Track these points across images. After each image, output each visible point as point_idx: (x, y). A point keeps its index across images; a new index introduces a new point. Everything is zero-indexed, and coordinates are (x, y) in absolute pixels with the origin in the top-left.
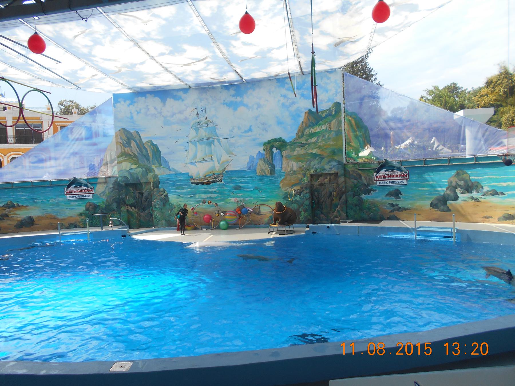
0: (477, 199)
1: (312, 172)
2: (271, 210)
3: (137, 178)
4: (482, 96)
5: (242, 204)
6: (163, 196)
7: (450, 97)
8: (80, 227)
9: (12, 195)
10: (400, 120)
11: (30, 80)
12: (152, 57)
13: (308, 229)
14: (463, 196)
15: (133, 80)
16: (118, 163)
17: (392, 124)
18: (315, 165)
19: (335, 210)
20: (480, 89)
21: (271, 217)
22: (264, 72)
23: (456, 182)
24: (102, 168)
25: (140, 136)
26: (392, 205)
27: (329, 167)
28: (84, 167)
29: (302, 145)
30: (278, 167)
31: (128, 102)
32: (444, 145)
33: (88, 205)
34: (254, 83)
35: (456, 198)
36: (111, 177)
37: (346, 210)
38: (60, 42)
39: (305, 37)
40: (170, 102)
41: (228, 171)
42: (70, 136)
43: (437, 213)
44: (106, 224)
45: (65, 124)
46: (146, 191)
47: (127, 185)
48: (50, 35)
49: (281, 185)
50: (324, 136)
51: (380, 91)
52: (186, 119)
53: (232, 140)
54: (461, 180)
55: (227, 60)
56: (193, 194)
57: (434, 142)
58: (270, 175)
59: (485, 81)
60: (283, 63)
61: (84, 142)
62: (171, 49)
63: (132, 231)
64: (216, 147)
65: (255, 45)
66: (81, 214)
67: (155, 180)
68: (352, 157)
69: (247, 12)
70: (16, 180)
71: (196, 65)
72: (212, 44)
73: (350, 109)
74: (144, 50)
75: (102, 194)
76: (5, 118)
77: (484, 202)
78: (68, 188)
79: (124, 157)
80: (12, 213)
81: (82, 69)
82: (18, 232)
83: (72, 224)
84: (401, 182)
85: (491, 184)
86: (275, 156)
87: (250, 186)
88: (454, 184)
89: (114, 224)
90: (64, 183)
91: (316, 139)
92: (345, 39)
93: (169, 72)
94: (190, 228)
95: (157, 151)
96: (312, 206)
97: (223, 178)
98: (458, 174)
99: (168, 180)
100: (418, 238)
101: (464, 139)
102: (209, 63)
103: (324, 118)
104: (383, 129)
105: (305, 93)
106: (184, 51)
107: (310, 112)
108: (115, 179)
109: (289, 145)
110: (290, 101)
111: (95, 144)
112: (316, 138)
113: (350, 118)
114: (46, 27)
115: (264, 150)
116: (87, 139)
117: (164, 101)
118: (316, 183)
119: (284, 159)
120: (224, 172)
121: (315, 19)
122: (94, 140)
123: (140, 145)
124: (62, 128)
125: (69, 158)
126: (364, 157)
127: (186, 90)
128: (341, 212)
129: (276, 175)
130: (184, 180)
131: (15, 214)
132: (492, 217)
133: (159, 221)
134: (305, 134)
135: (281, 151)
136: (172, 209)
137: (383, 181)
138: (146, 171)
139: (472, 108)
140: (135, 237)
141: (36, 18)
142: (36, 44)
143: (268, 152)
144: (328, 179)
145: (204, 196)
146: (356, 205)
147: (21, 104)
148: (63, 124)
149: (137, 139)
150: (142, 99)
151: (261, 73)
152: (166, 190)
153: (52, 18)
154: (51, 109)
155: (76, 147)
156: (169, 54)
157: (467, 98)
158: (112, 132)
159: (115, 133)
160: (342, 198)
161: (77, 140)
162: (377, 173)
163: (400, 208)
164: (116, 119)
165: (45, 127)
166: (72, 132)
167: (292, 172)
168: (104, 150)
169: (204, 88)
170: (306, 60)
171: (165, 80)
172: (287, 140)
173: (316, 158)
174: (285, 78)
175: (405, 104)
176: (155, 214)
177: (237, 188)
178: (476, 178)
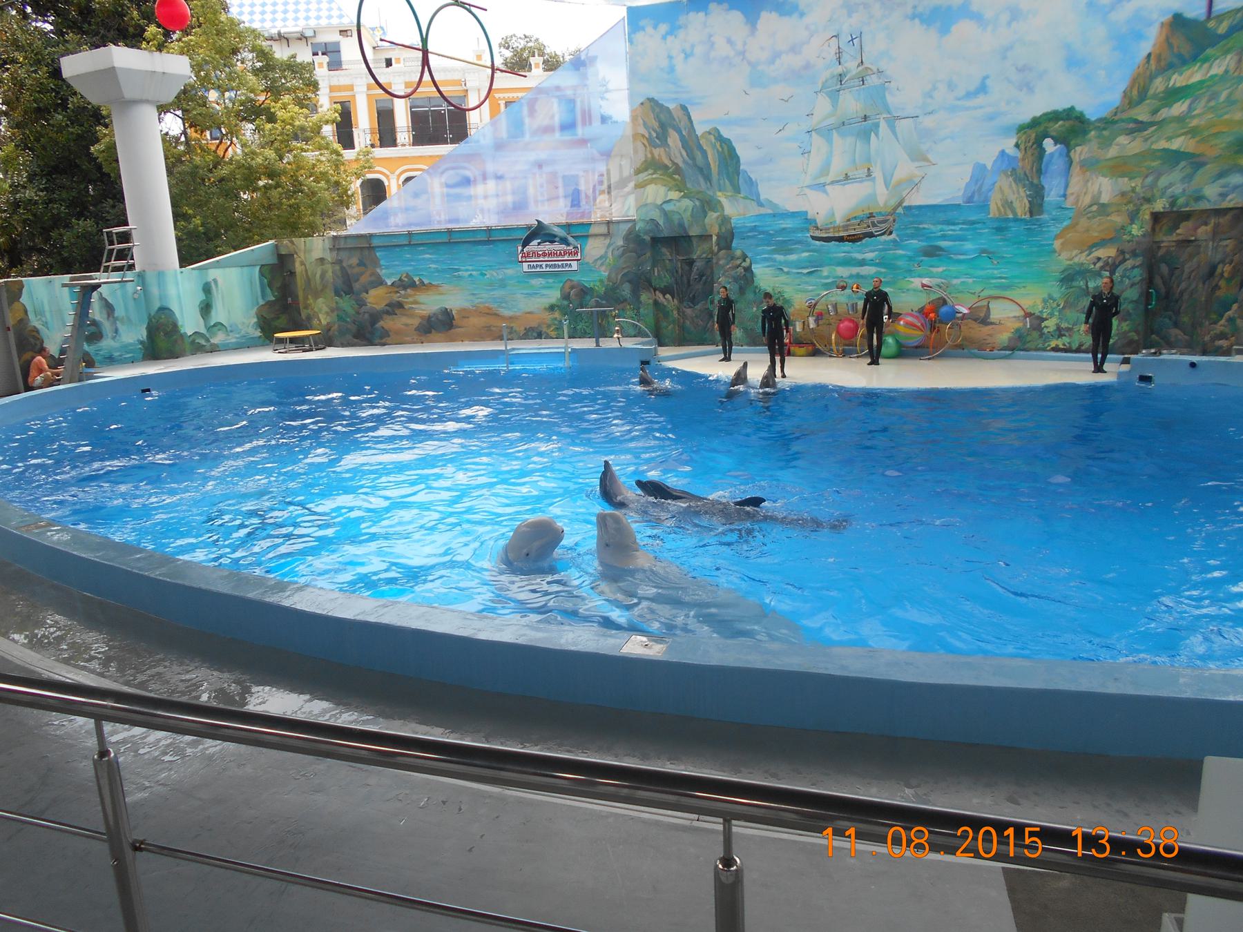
1: (1159, 206)
2: (1022, 313)
3: (681, 225)
6: (740, 270)
8: (548, 337)
13: (1125, 368)
16: (637, 186)
18: (1171, 185)
19: (1222, 316)
21: (1017, 330)
24: (600, 198)
25: (690, 118)
28: (558, 198)
29: (1139, 127)
31: (663, 28)
33: (568, 285)
36: (618, 222)
41: (909, 208)
42: (527, 120)
44: (604, 333)
45: (515, 95)
46: (699, 257)
47: (656, 241)
49: (1057, 244)
52: (807, 66)
53: (928, 122)
56: (814, 267)
61: (557, 135)
63: (664, 352)
66: (552, 308)
75: (599, 262)
78: (524, 246)
79: (650, 171)
80: (411, 299)
83: (532, 329)
87: (969, 246)
94: (803, 350)
95: (729, 157)
96: (1148, 302)
97: (896, 226)
99: (754, 229)
108: (630, 225)
109: (1096, 128)
111: (583, 142)
115: (1017, 146)
118: (1167, 240)
119: (1076, 169)
120: (900, 210)
122: (580, 131)
123: (691, 143)
124: (507, 104)
129: (1045, 217)
130: (794, 231)
131: (416, 302)
135: (1069, 151)
140: (670, 364)
143: (1029, 153)
144: (1209, 228)
149: (683, 124)
152: (749, 255)
159: (632, 111)
161: (548, 130)
164: (633, 74)
165: (472, 101)
166: (532, 112)
167: (1094, 208)
168: (607, 155)
172: (1092, 114)
173: (1178, 164)
177: (933, 252)
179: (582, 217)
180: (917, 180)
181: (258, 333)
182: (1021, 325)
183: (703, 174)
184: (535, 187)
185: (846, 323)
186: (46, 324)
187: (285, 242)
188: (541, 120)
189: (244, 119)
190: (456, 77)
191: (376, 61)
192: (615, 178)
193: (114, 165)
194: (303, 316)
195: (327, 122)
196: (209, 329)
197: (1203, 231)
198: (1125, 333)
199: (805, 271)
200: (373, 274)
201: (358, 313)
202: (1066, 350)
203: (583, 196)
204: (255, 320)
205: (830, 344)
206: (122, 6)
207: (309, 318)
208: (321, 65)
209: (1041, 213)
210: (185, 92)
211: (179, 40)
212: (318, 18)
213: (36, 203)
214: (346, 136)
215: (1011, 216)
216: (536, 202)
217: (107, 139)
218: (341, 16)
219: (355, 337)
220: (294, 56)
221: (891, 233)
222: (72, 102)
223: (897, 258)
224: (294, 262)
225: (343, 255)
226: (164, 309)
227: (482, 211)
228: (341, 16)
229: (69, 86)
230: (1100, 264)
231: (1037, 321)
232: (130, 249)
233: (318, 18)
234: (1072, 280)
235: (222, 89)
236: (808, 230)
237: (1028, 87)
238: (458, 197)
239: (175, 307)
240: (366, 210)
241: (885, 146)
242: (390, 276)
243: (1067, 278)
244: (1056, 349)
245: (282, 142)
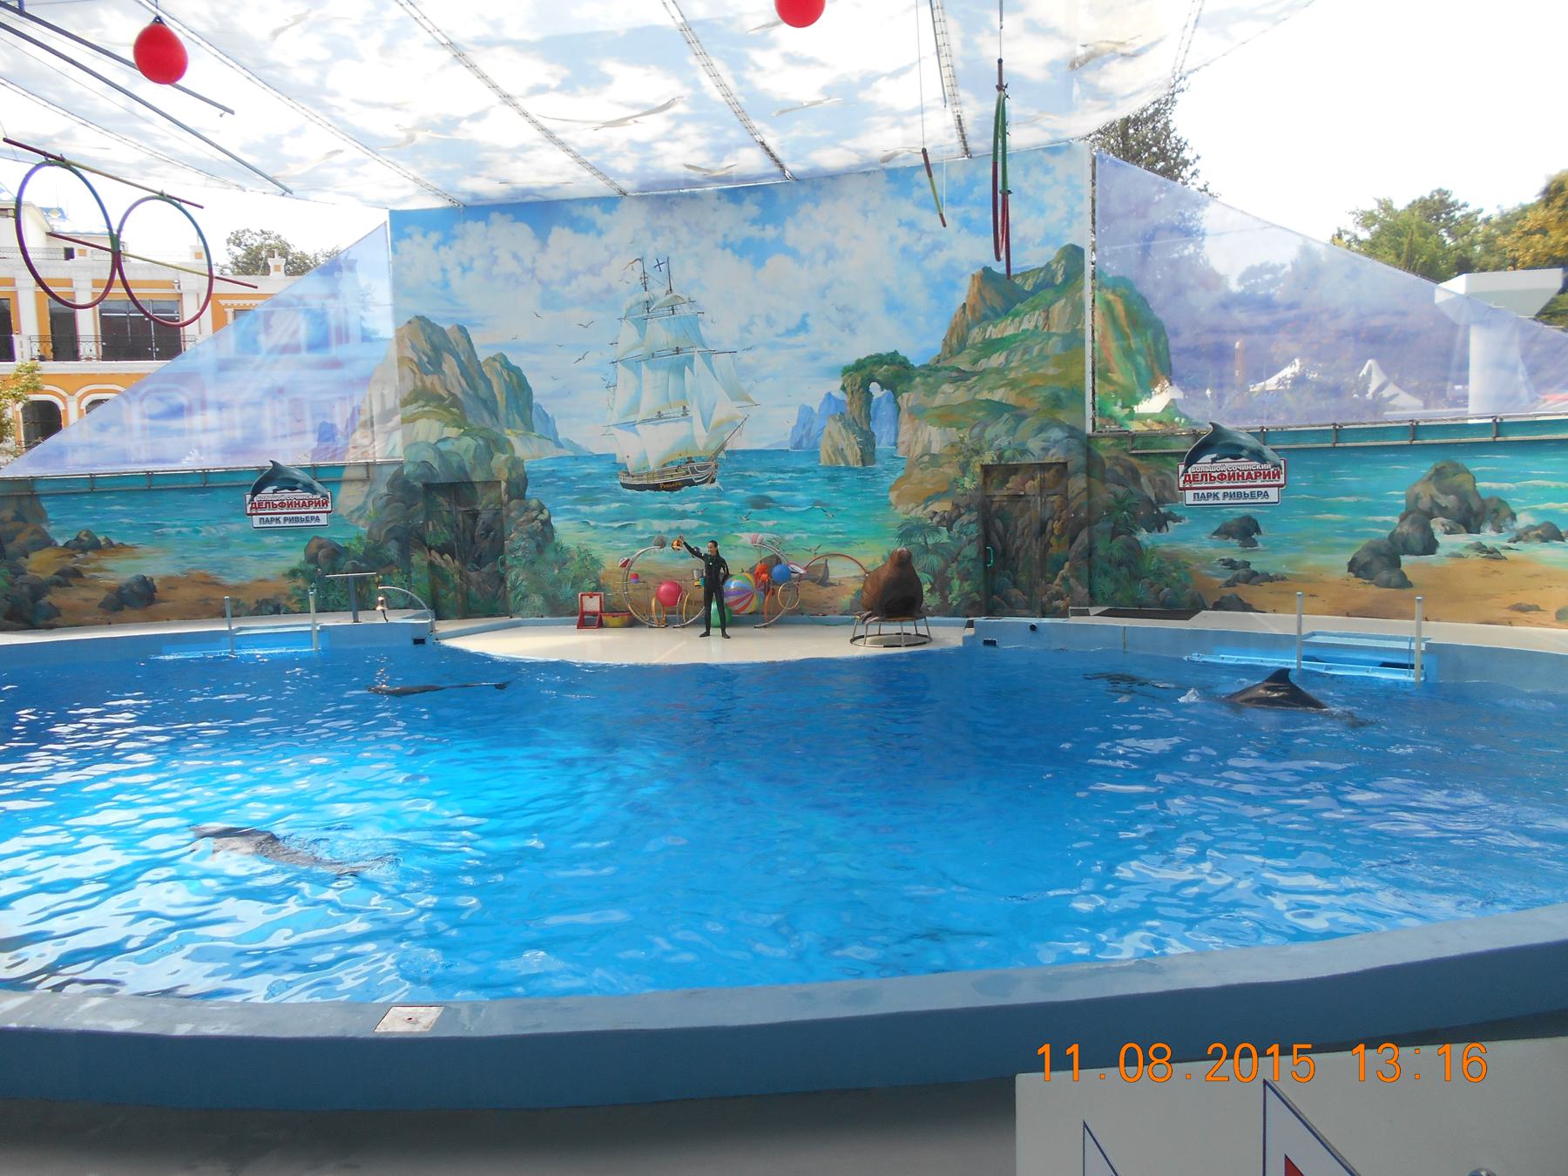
0: (1493, 551)
1: (989, 458)
3: (462, 468)
4: (1529, 233)
6: (537, 524)
7: (1426, 233)
8: (289, 612)
9: (90, 513)
10: (1267, 304)
11: (143, 168)
12: (507, 98)
13: (971, 631)
14: (1451, 543)
15: (448, 167)
16: (404, 421)
17: (1241, 317)
18: (997, 437)
20: (1525, 209)
23: (1432, 498)
24: (358, 435)
25: (469, 341)
26: (1230, 564)
27: (1041, 445)
28: (302, 433)
29: (962, 376)
30: (884, 440)
31: (435, 237)
32: (1399, 384)
34: (820, 184)
35: (1430, 547)
36: (382, 464)
37: (1090, 577)
38: (228, 47)
39: (979, 40)
40: (561, 237)
41: (733, 453)
42: (262, 338)
43: (1369, 592)
44: (365, 604)
45: (248, 302)
46: (485, 508)
47: (430, 488)
48: (201, 27)
49: (892, 496)
51: (1207, 211)
52: (609, 290)
53: (746, 358)
54: (1446, 493)
55: (736, 108)
56: (626, 520)
57: (1369, 372)
58: (860, 466)
59: (1542, 184)
60: (907, 120)
61: (306, 356)
63: (443, 627)
64: (698, 378)
65: (823, 65)
66: (293, 573)
67: (514, 474)
68: (1111, 417)
71: (640, 125)
72: (692, 60)
73: (1112, 268)
74: (483, 77)
76: (69, 283)
77: (1514, 562)
78: (254, 494)
79: (421, 403)
80: (93, 565)
81: (297, 133)
82: (109, 623)
83: (266, 602)
84: (1259, 494)
85: (1541, 507)
86: (877, 408)
87: (800, 497)
88: (1425, 503)
89: (391, 605)
90: (246, 479)
91: (1002, 359)
92: (1104, 45)
93: (561, 144)
94: (616, 621)
95: (519, 388)
96: (986, 561)
98: (1439, 473)
99: (552, 474)
100: (1306, 665)
101: (1464, 366)
102: (680, 120)
103: (1032, 293)
104: (1214, 330)
106: (607, 80)
107: (987, 275)
108: (395, 468)
110: (927, 240)
111: (336, 364)
113: (1111, 297)
115: (843, 388)
116: (312, 347)
117: (542, 236)
118: (999, 494)
119: (904, 417)
120: (722, 455)
122: (335, 351)
123: (471, 370)
124: (238, 312)
125: (258, 404)
126: (1151, 416)
127: (608, 203)
128: (1072, 581)
129: (878, 466)
130: (600, 477)
131: (101, 569)
132: (1537, 608)
133: (525, 597)
134: (970, 342)
137: (1205, 491)
138: (488, 447)
139: (1497, 268)
142: (159, 55)
143: (857, 396)
144: (1036, 483)
145: (660, 526)
146: (1120, 564)
147: (115, 239)
148: (242, 302)
149: (462, 347)
150: (475, 228)
152: (547, 505)
155: (280, 373)
156: (559, 89)
157: (1480, 238)
158: (384, 324)
161: (285, 349)
162: (1188, 465)
163: (1255, 574)
164: (398, 287)
165: (189, 309)
166: (267, 327)
167: (926, 458)
168: (366, 381)
169: (666, 198)
170: (978, 110)
171: (548, 172)
172: (916, 361)
175: (1284, 255)
176: (512, 576)
177: (761, 503)
178: (1494, 485)
179: (333, 457)
183: (487, 409)
184: (271, 417)
188: (280, 336)
191: (48, 250)
192: (376, 410)
197: (1031, 486)
198: (968, 594)
199: (616, 525)
200: (37, 532)
201: (12, 584)
205: (649, 611)
209: (873, 462)
219: (8, 617)
223: (722, 509)
227: (200, 448)
230: (937, 519)
237: (850, 328)
242: (61, 534)
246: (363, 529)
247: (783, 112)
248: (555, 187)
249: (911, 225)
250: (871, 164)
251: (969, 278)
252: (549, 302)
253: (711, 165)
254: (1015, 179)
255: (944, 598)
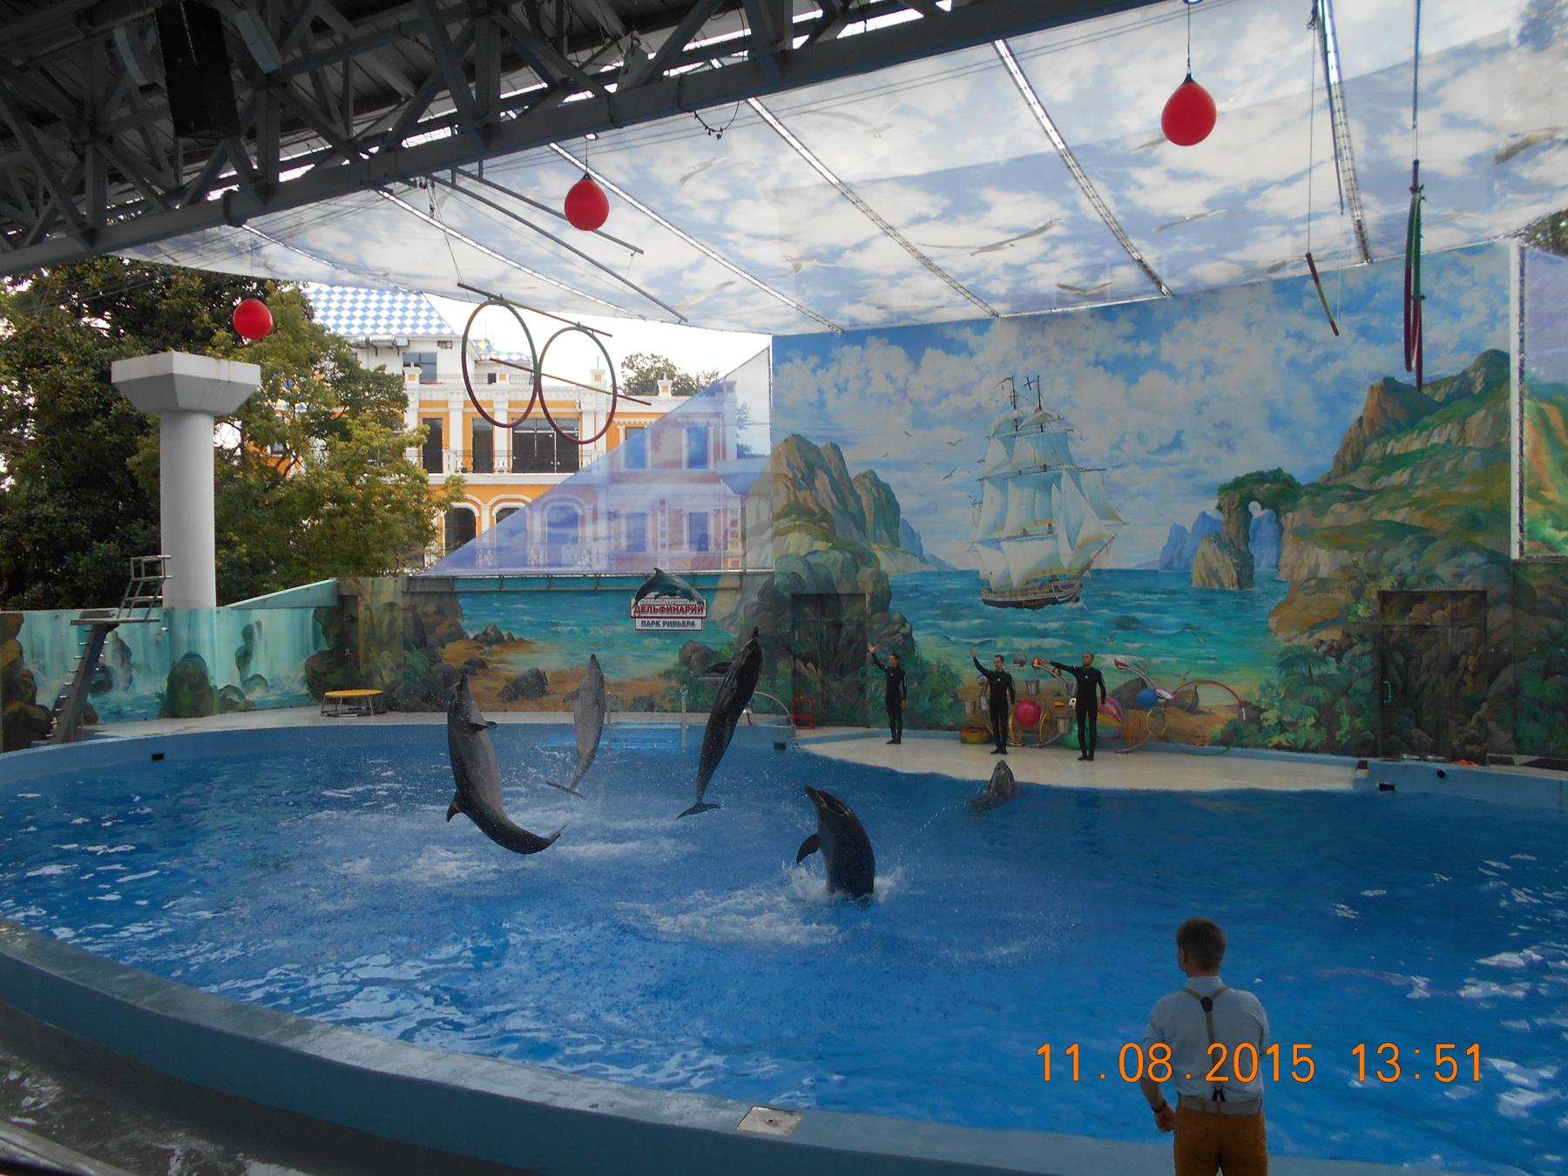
1: (1387, 584)
2: (1235, 702)
3: (829, 581)
5: (1138, 674)
9: (499, 610)
12: (889, 230)
13: (1362, 773)
15: (830, 294)
16: (775, 534)
18: (1398, 561)
19: (1470, 717)
21: (1232, 722)
22: (1232, 262)
27: (1449, 571)
28: (681, 543)
29: (1356, 495)
30: (1264, 562)
31: (814, 360)
34: (1199, 300)
36: (754, 574)
39: (1386, 140)
40: (933, 358)
41: (1098, 572)
42: (649, 454)
47: (797, 598)
48: (622, 179)
49: (1272, 622)
50: (1437, 467)
52: (979, 408)
53: (1117, 476)
56: (987, 635)
58: (1236, 588)
60: (1299, 227)
61: (685, 468)
62: (946, 202)
63: (803, 734)
65: (1208, 178)
66: (668, 674)
69: (1189, 77)
70: (509, 571)
72: (1071, 183)
74: (867, 211)
76: (491, 404)
78: (638, 599)
81: (695, 267)
83: (642, 699)
87: (1169, 619)
91: (1405, 476)
93: (938, 271)
94: (975, 737)
95: (887, 503)
96: (1383, 697)
97: (1084, 591)
99: (915, 588)
102: (1056, 242)
105: (1375, 322)
107: (1389, 386)
108: (766, 579)
109: (1308, 493)
110: (1319, 351)
111: (715, 478)
112: (1408, 471)
113: (1544, 406)
114: (608, 159)
115: (1219, 508)
117: (915, 356)
118: (1399, 624)
119: (1288, 538)
120: (1087, 574)
121: (1426, 77)
122: (711, 466)
123: (842, 485)
127: (980, 326)
129: (1256, 589)
131: (502, 661)
134: (1366, 458)
135: (1278, 517)
136: (922, 678)
138: (855, 560)
141: (591, 136)
143: (1234, 515)
144: (1445, 613)
145: (1021, 643)
150: (851, 352)
151: (1222, 264)
153: (631, 136)
154: (608, 377)
155: (665, 489)
156: (939, 218)
160: (1499, 680)
164: (778, 408)
166: (656, 444)
167: (1313, 582)
169: (1038, 320)
173: (1404, 537)
174: (1303, 279)
177: (1127, 624)
180: (1106, 541)
181: (304, 690)
182: (1234, 716)
185: (1026, 706)
186: (43, 669)
187: (349, 581)
189: (314, 434)
190: (569, 397)
191: (476, 376)
192: (751, 521)
193: (152, 479)
194: (363, 671)
195: (411, 444)
196: (245, 682)
202: (1290, 749)
203: (712, 542)
204: (303, 674)
206: (192, 307)
207: (369, 675)
208: (412, 377)
209: (1251, 584)
210: (248, 402)
211: (249, 346)
212: (415, 326)
213: (54, 519)
214: (433, 460)
215: (1217, 587)
216: (656, 547)
217: (147, 450)
218: (440, 326)
220: (382, 368)
221: (1077, 600)
222: (116, 407)
224: (357, 605)
225: (418, 600)
226: (193, 657)
227: (590, 553)
228: (440, 326)
229: (115, 390)
230: (1323, 648)
231: (1256, 711)
232: (158, 584)
233: (415, 326)
234: (1293, 665)
235: (292, 400)
236: (980, 593)
238: (563, 539)
239: (206, 655)
240: (451, 547)
241: (1068, 500)
242: (472, 628)
243: (1288, 662)
244: (1279, 747)
245: (354, 463)
246: (734, 636)
247: (1162, 228)
248: (930, 310)
249: (1299, 336)
250: (1259, 273)
251: (1367, 388)
252: (921, 420)
253: (1086, 284)
254: (1428, 283)
255: (1331, 734)
